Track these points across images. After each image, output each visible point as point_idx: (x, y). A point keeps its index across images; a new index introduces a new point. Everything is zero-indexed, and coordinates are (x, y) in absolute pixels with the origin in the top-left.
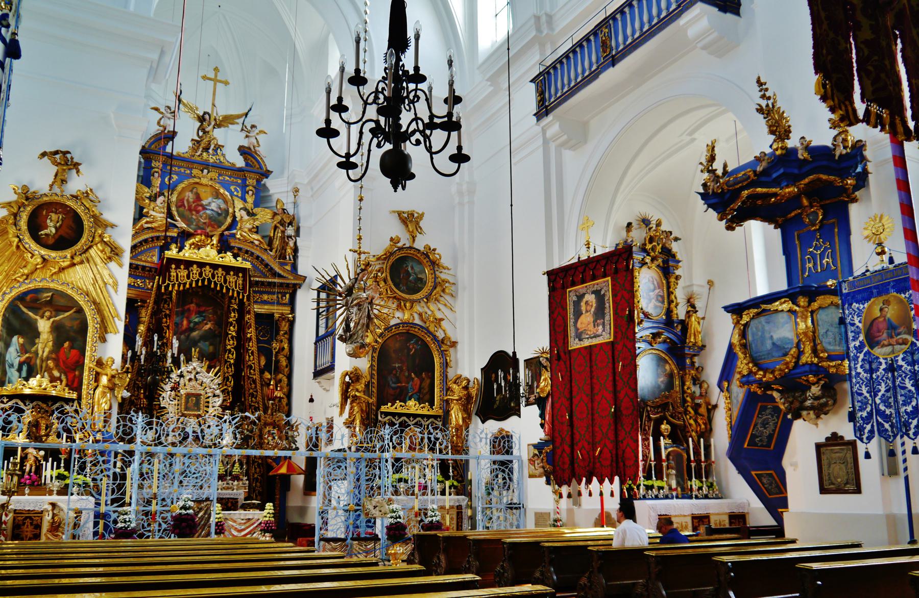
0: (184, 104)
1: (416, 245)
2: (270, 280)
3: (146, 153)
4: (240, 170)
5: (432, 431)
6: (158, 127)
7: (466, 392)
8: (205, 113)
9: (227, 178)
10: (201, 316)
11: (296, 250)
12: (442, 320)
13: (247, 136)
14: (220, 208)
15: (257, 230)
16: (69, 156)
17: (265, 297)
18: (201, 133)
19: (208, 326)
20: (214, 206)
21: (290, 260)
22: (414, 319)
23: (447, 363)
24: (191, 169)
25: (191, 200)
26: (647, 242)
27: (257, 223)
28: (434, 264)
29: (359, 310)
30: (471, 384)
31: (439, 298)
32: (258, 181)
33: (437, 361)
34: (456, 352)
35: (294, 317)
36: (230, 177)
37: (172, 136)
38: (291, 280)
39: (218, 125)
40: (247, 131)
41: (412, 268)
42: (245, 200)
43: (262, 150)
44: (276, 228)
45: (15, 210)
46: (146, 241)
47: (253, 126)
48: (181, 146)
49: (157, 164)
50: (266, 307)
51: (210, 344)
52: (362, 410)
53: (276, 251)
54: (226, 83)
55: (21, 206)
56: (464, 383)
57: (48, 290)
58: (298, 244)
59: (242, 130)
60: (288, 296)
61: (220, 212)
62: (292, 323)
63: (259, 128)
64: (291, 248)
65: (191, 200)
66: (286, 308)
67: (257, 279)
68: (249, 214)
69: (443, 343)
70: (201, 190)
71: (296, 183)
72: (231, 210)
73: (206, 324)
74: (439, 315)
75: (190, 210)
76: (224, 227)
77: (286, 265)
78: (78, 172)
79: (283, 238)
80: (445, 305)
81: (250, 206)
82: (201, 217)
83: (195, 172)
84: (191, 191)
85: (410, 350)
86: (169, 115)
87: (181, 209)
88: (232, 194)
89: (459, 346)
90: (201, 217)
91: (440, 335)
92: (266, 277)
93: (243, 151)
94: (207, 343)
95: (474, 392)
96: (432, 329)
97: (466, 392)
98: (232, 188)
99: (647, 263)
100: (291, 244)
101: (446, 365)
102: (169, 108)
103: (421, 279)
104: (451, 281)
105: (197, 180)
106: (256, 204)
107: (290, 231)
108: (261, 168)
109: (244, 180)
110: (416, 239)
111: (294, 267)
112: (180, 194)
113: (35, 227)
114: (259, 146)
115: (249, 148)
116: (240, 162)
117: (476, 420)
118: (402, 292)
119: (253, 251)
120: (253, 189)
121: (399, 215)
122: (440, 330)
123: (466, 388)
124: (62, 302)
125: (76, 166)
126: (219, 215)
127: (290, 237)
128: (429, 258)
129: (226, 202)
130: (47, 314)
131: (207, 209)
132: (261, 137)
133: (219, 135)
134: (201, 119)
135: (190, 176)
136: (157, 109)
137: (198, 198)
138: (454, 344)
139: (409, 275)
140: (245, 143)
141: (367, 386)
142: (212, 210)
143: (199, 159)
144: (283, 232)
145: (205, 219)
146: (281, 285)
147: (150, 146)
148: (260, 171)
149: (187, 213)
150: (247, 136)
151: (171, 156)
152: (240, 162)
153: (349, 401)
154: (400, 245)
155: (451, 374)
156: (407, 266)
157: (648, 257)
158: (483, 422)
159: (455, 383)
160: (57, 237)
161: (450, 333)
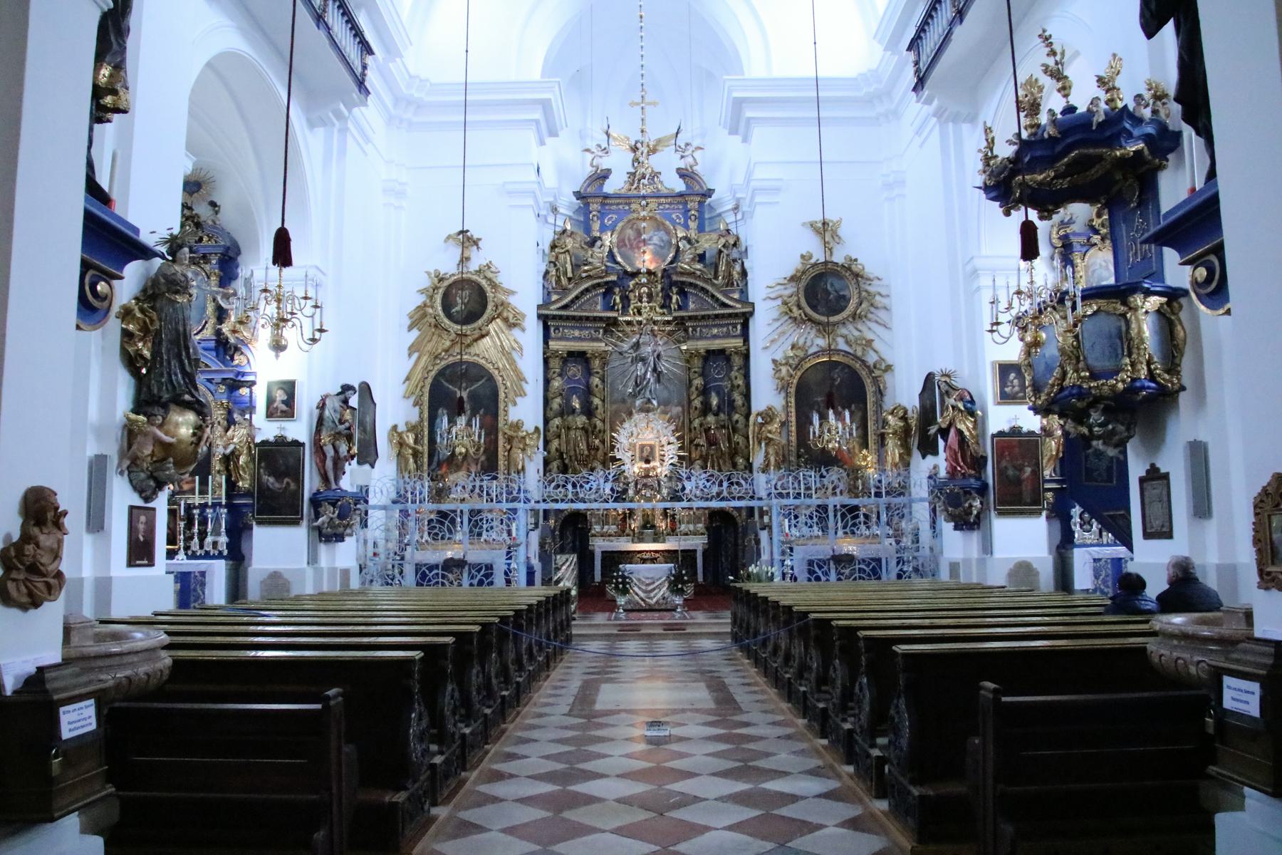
0: (615, 139)
1: (835, 259)
2: (717, 312)
3: (584, 197)
4: (681, 195)
5: (825, 473)
6: (591, 169)
7: (902, 424)
8: (636, 142)
9: (667, 206)
11: (744, 273)
12: (872, 340)
13: (682, 157)
15: (701, 258)
16: (469, 234)
17: (715, 331)
18: (636, 164)
21: (738, 285)
22: (837, 344)
23: (880, 390)
24: (629, 204)
25: (632, 238)
26: (1094, 217)
27: (700, 251)
28: (857, 275)
29: (644, 364)
30: (910, 414)
31: (870, 316)
32: (701, 203)
33: (870, 389)
34: (893, 376)
35: (748, 350)
36: (670, 204)
37: (603, 176)
38: (739, 308)
39: (653, 151)
40: (682, 151)
41: (832, 285)
42: (687, 227)
43: (697, 169)
44: (720, 252)
45: (430, 294)
46: (587, 290)
47: (687, 145)
48: (613, 185)
49: (595, 207)
52: (777, 454)
53: (723, 278)
54: (655, 104)
55: (435, 288)
56: (901, 413)
57: (461, 362)
58: (746, 265)
59: (676, 151)
62: (746, 357)
63: (695, 144)
64: (738, 273)
65: (632, 238)
66: (738, 340)
67: (703, 313)
68: (689, 241)
69: (875, 367)
71: (738, 200)
72: (674, 241)
74: (870, 336)
76: (669, 259)
77: (733, 292)
78: (478, 248)
79: (728, 264)
80: (877, 322)
81: (693, 234)
83: (634, 206)
84: (632, 228)
85: (834, 380)
86: (600, 154)
87: (623, 249)
88: (673, 222)
89: (897, 369)
91: (871, 358)
92: (715, 309)
93: (684, 174)
95: (913, 423)
96: (859, 353)
97: (902, 424)
98: (674, 216)
99: (1095, 244)
100: (738, 268)
101: (880, 393)
102: (599, 146)
103: (844, 297)
104: (883, 292)
105: (635, 215)
106: (701, 229)
107: (735, 254)
108: (701, 187)
109: (686, 203)
110: (834, 251)
111: (744, 292)
112: (620, 233)
113: (447, 306)
114: (697, 164)
115: (687, 170)
116: (679, 186)
117: (916, 454)
118: (823, 314)
120: (696, 214)
121: (812, 225)
122: (872, 353)
123: (904, 418)
124: (473, 371)
125: (476, 243)
126: (660, 246)
127: (735, 261)
128: (850, 272)
129: (668, 232)
130: (464, 385)
132: (698, 154)
133: (655, 162)
134: (634, 149)
135: (630, 211)
136: (588, 150)
138: (889, 368)
139: (829, 293)
140: (682, 164)
141: (783, 424)
143: (635, 192)
144: (728, 255)
146: (730, 316)
147: (586, 190)
148: (701, 191)
150: (682, 157)
151: (606, 197)
152: (679, 186)
153: (763, 445)
154: (813, 261)
155: (888, 404)
156: (826, 284)
157: (1096, 237)
158: (924, 457)
159: (892, 413)
160: (465, 313)
161: (883, 357)
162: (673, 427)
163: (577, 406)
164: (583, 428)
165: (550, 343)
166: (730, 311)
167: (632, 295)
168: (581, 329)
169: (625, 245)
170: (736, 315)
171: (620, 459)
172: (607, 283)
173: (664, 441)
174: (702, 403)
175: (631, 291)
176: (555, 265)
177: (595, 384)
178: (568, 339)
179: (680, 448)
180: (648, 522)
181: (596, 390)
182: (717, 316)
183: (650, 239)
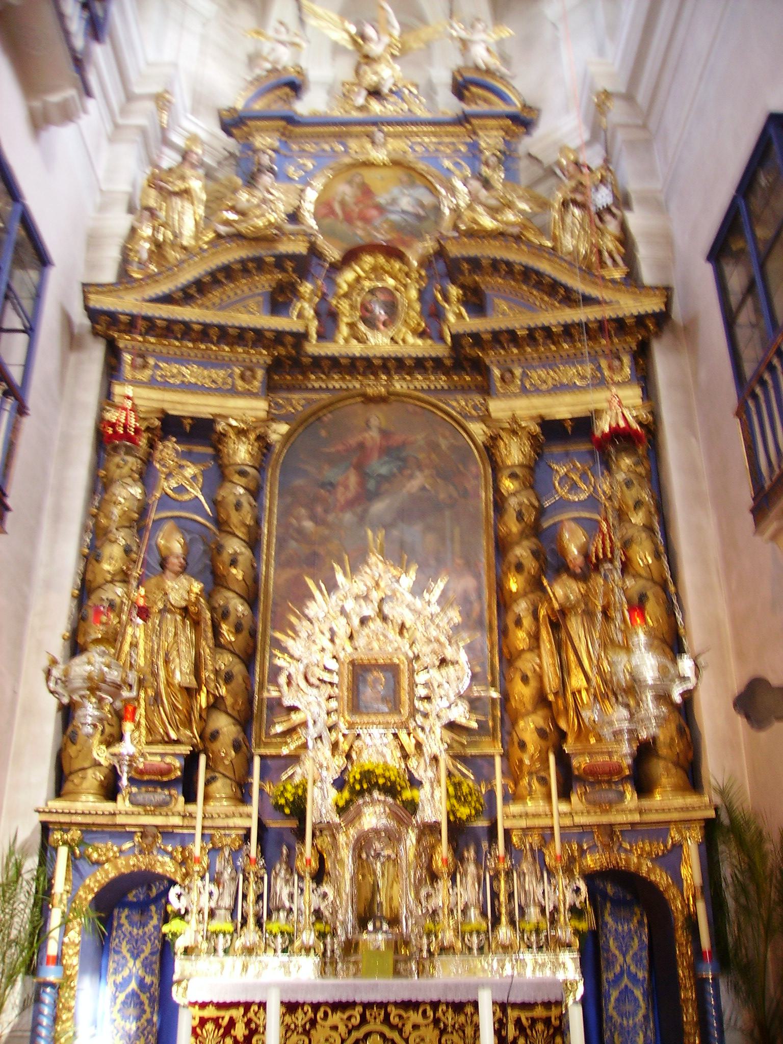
14: (422, 206)
20: (406, 203)
61: (422, 213)
65: (349, 199)
70: (372, 177)
73: (411, 477)
75: (348, 218)
90: (377, 229)
137: (366, 191)
142: (404, 212)
149: (343, 227)
164: (185, 611)
165: (119, 390)
167: (344, 306)
168: (206, 363)
169: (332, 212)
170: (620, 324)
172: (280, 261)
174: (536, 554)
177: (231, 500)
181: (235, 518)
182: (568, 330)
183: (394, 201)
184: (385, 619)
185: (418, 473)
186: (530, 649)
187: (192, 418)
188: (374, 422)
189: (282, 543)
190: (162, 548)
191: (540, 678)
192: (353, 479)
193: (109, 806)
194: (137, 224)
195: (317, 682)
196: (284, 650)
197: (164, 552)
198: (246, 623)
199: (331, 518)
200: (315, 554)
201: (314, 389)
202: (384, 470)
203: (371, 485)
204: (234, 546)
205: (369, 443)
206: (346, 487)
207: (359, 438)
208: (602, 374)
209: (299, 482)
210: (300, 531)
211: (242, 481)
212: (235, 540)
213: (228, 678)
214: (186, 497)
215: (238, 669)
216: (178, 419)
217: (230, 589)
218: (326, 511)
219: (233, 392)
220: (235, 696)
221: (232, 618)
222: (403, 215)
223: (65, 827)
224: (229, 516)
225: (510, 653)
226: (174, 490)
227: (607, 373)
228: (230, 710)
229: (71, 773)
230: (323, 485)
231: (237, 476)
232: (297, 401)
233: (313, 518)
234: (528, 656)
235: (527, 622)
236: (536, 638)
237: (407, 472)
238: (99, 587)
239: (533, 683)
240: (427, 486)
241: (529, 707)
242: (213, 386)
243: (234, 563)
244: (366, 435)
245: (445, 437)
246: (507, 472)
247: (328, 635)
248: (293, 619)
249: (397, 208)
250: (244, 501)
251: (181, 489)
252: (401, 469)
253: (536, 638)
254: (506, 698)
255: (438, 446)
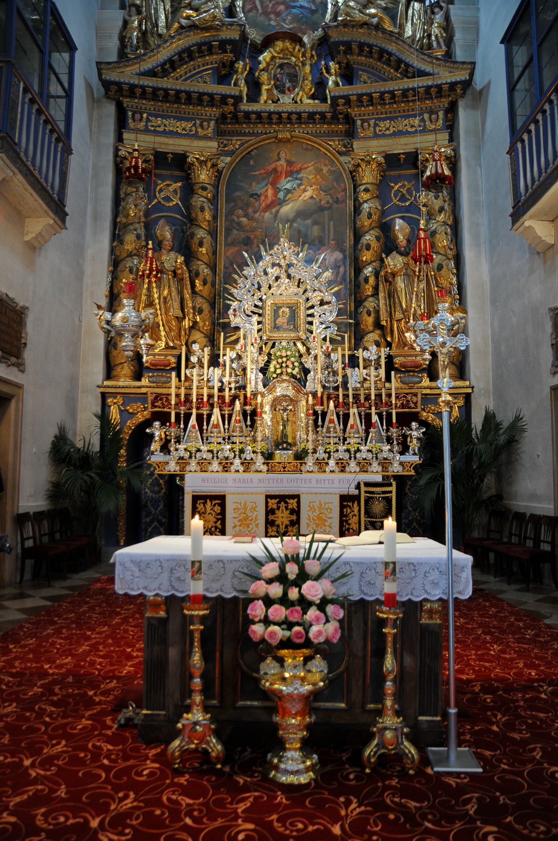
10: (297, 179)
19: (308, 194)
50: (404, 140)
51: (315, 223)
60: (441, 114)
61: (313, 8)
73: (305, 191)
75: (266, 13)
82: (284, 20)
87: (251, 14)
90: (284, 20)
94: (309, 222)
119: (371, 41)
126: (313, 12)
131: (294, 7)
142: (301, 7)
145: (291, 23)
149: (262, 19)
162: (328, 274)
163: (168, 235)
165: (125, 136)
166: (430, 82)
167: (264, 77)
171: (237, 329)
172: (223, 44)
173: (315, 298)
174: (378, 238)
175: (263, 70)
176: (139, 12)
177: (199, 204)
178: (156, 133)
179: (340, 313)
180: (284, 435)
181: (200, 216)
184: (289, 276)
185: (308, 188)
186: (372, 296)
187: (172, 154)
188: (283, 155)
189: (228, 231)
190: (159, 235)
191: (377, 312)
192: (270, 192)
193: (137, 384)
194: (127, 18)
195: (250, 314)
196: (233, 296)
197: (160, 238)
198: (209, 280)
199: (257, 215)
200: (248, 238)
201: (245, 134)
202: (288, 186)
203: (281, 195)
204: (201, 234)
205: (279, 169)
206: (266, 197)
207: (273, 166)
208: (425, 125)
209: (238, 194)
210: (239, 224)
211: (204, 193)
212: (201, 229)
213: (200, 312)
214: (171, 204)
215: (206, 307)
216: (164, 154)
217: (199, 260)
218: (255, 212)
219: (196, 136)
220: (204, 321)
221: (201, 277)
222: (301, 10)
223: (114, 395)
224: (197, 215)
225: (361, 297)
226: (163, 199)
227: (428, 123)
228: (201, 330)
229: (115, 366)
230: (252, 196)
231: (200, 190)
232: (236, 143)
233: (246, 215)
234: (371, 299)
235: (372, 280)
236: (376, 288)
237: (302, 187)
238: (123, 260)
239: (373, 315)
240: (314, 196)
241: (371, 328)
242: (184, 132)
243: (201, 244)
244: (278, 163)
245: (326, 165)
246: (362, 188)
247: (256, 286)
248: (236, 277)
249: (298, 4)
250: (206, 206)
251: (167, 199)
252: (299, 185)
253: (376, 288)
254: (357, 324)
255: (322, 170)
